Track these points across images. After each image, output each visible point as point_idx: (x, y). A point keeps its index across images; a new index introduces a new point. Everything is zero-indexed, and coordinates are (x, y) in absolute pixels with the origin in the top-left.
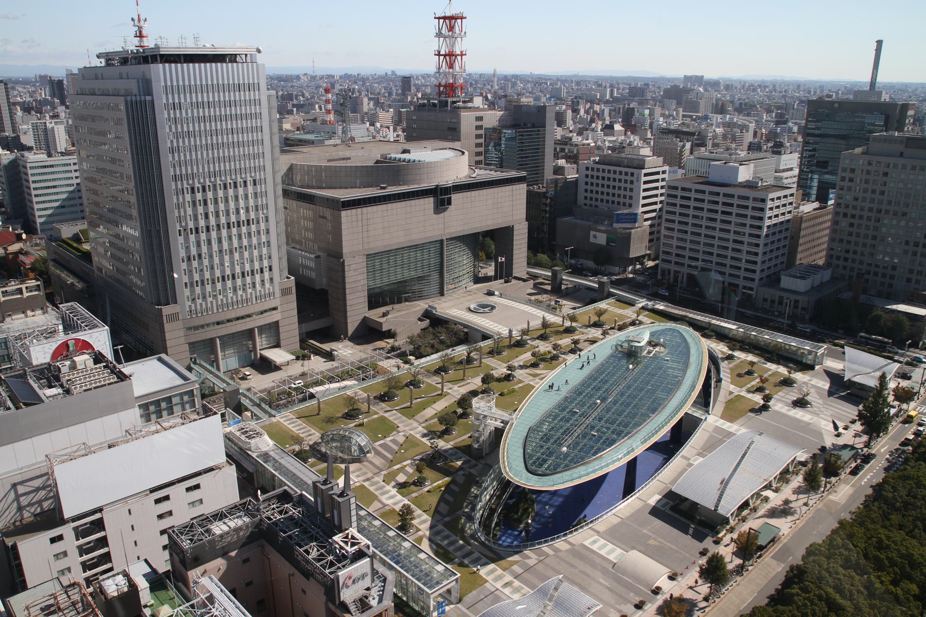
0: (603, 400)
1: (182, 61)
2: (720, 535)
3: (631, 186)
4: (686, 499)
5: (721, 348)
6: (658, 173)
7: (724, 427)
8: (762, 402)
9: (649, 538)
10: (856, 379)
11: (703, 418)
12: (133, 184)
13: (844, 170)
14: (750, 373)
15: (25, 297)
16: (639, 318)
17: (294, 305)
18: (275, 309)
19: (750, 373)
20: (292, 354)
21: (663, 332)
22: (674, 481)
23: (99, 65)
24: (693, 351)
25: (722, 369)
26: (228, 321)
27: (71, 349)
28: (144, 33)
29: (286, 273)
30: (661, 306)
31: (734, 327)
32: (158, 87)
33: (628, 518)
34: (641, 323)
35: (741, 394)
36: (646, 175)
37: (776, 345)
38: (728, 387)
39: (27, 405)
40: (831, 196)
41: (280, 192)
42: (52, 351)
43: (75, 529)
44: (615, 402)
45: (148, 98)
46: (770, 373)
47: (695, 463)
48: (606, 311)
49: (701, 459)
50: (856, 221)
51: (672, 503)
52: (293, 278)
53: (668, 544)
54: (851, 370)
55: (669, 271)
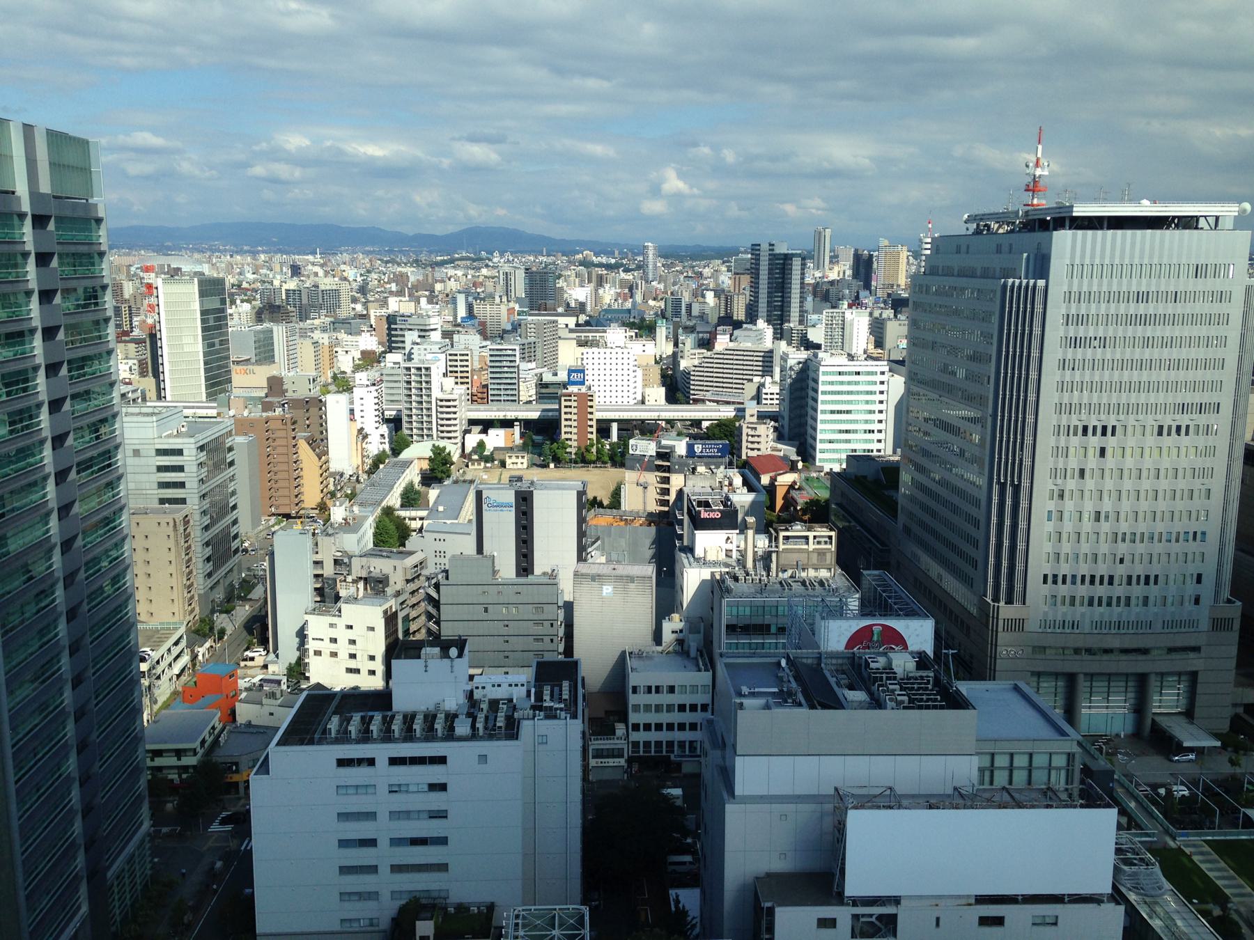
1: (1105, 226)
12: (990, 411)
15: (811, 549)
17: (1234, 651)
18: (1196, 649)
20: (1217, 736)
23: (964, 232)
26: (1107, 651)
27: (875, 638)
28: (1042, 183)
29: (1226, 593)
32: (1058, 266)
39: (825, 706)
41: (1239, 453)
42: (849, 635)
43: (856, 917)
45: (1041, 283)
52: (1239, 603)
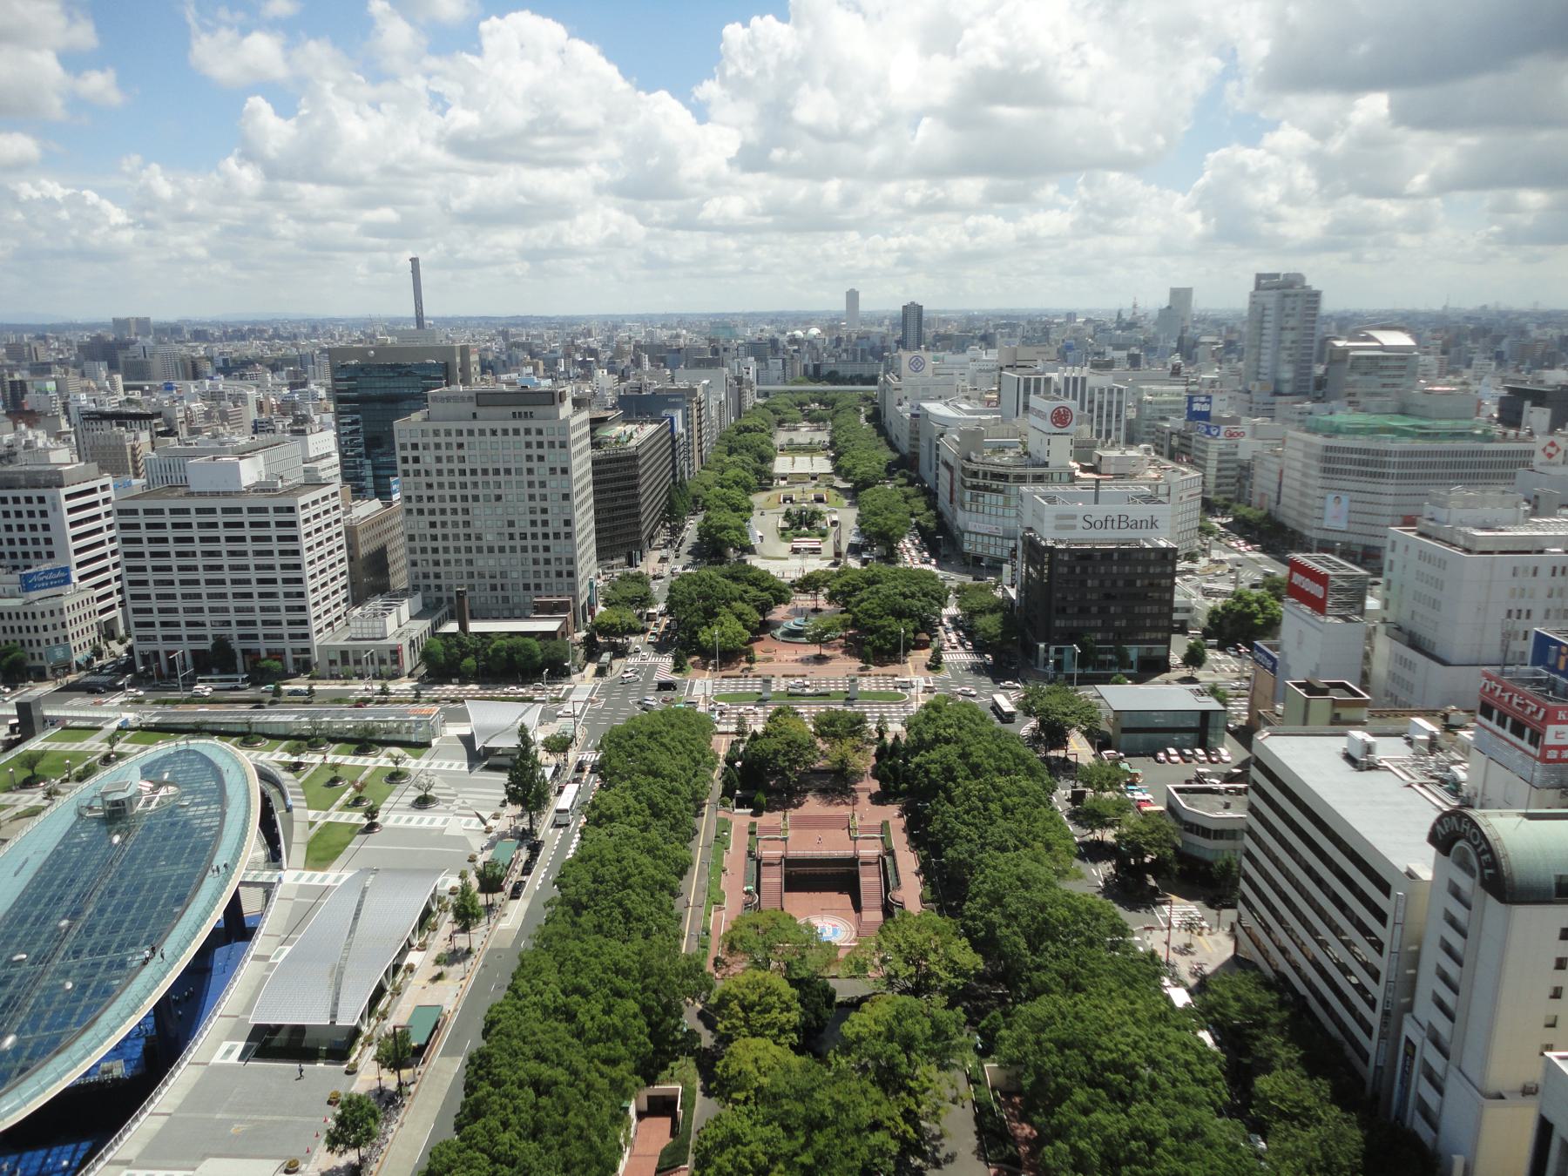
0: (74, 915)
2: (352, 1060)
3: (44, 521)
4: (279, 1028)
5: (275, 757)
6: (93, 491)
7: (315, 882)
8: (365, 822)
9: (229, 1123)
10: (491, 744)
11: (275, 880)
13: (403, 447)
14: (333, 782)
16: (115, 749)
19: (333, 782)
21: (166, 760)
22: (248, 1009)
24: (227, 778)
25: (288, 791)
30: (152, 715)
31: (291, 718)
33: (180, 1109)
34: (120, 756)
35: (330, 819)
36: (68, 497)
37: (366, 729)
38: (303, 819)
40: (394, 487)
44: (101, 911)
46: (367, 772)
47: (279, 960)
48: (42, 754)
49: (288, 949)
50: (438, 518)
51: (256, 1044)
53: (268, 1118)
54: (483, 731)
55: (156, 654)
